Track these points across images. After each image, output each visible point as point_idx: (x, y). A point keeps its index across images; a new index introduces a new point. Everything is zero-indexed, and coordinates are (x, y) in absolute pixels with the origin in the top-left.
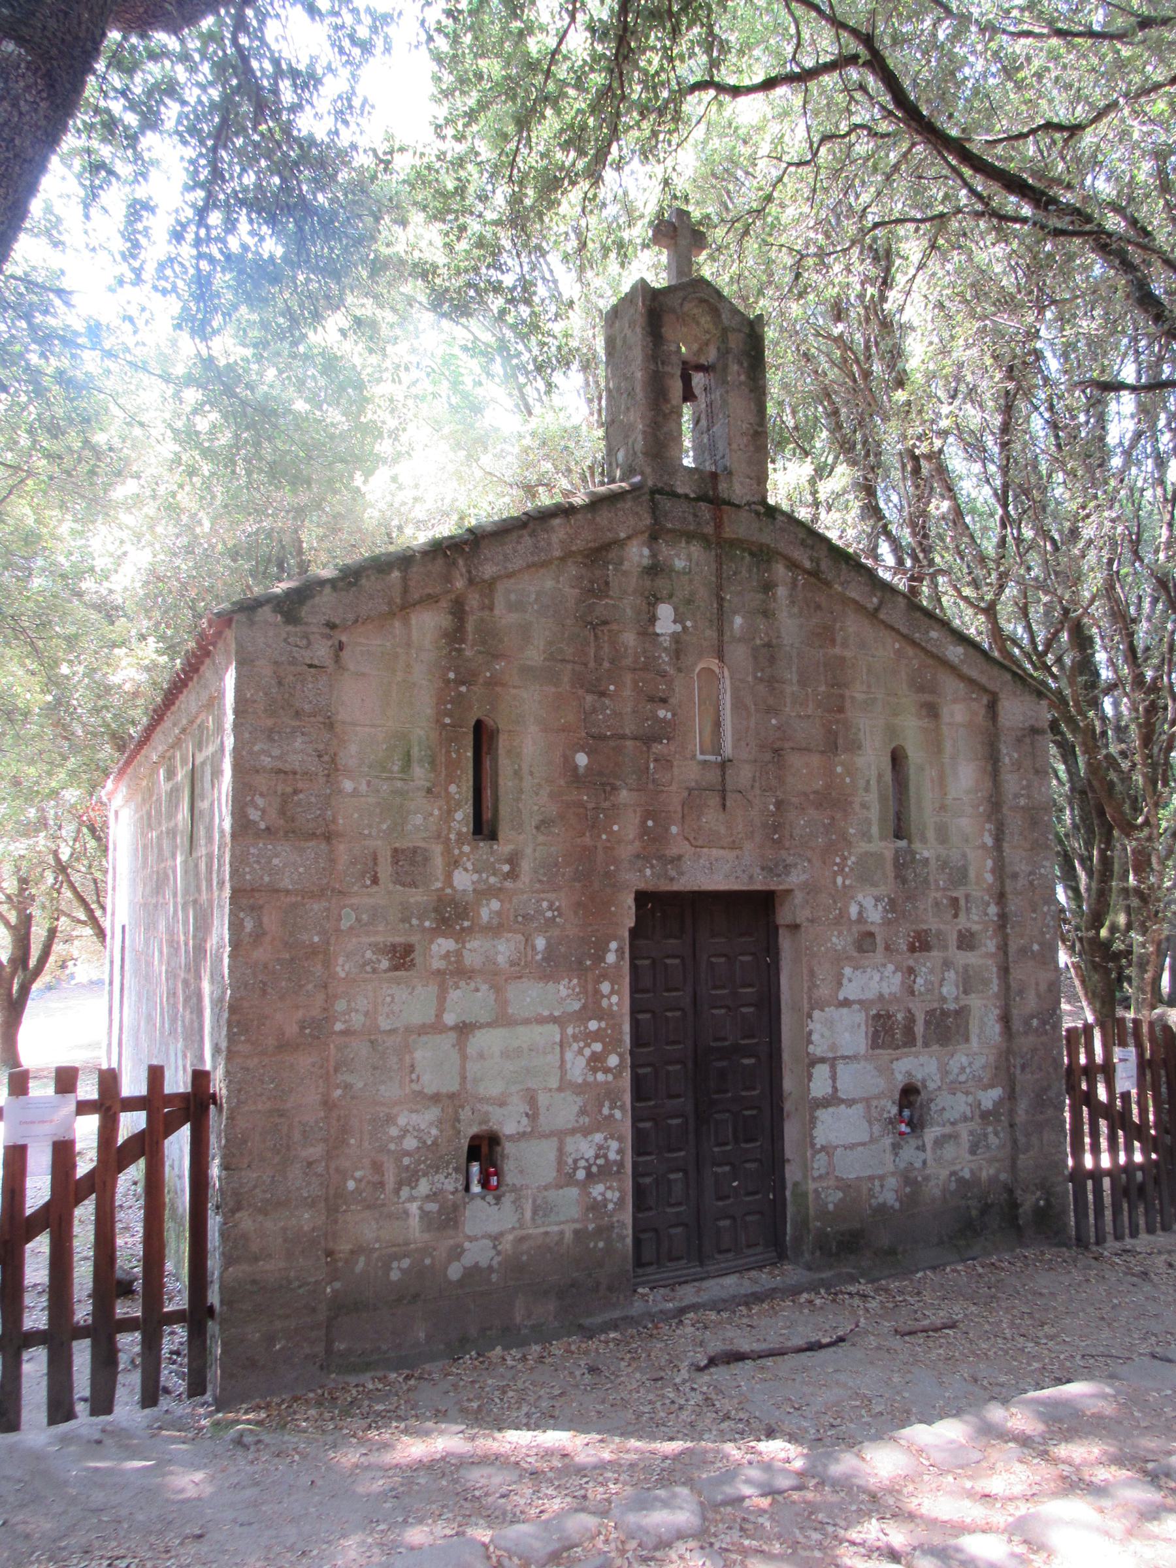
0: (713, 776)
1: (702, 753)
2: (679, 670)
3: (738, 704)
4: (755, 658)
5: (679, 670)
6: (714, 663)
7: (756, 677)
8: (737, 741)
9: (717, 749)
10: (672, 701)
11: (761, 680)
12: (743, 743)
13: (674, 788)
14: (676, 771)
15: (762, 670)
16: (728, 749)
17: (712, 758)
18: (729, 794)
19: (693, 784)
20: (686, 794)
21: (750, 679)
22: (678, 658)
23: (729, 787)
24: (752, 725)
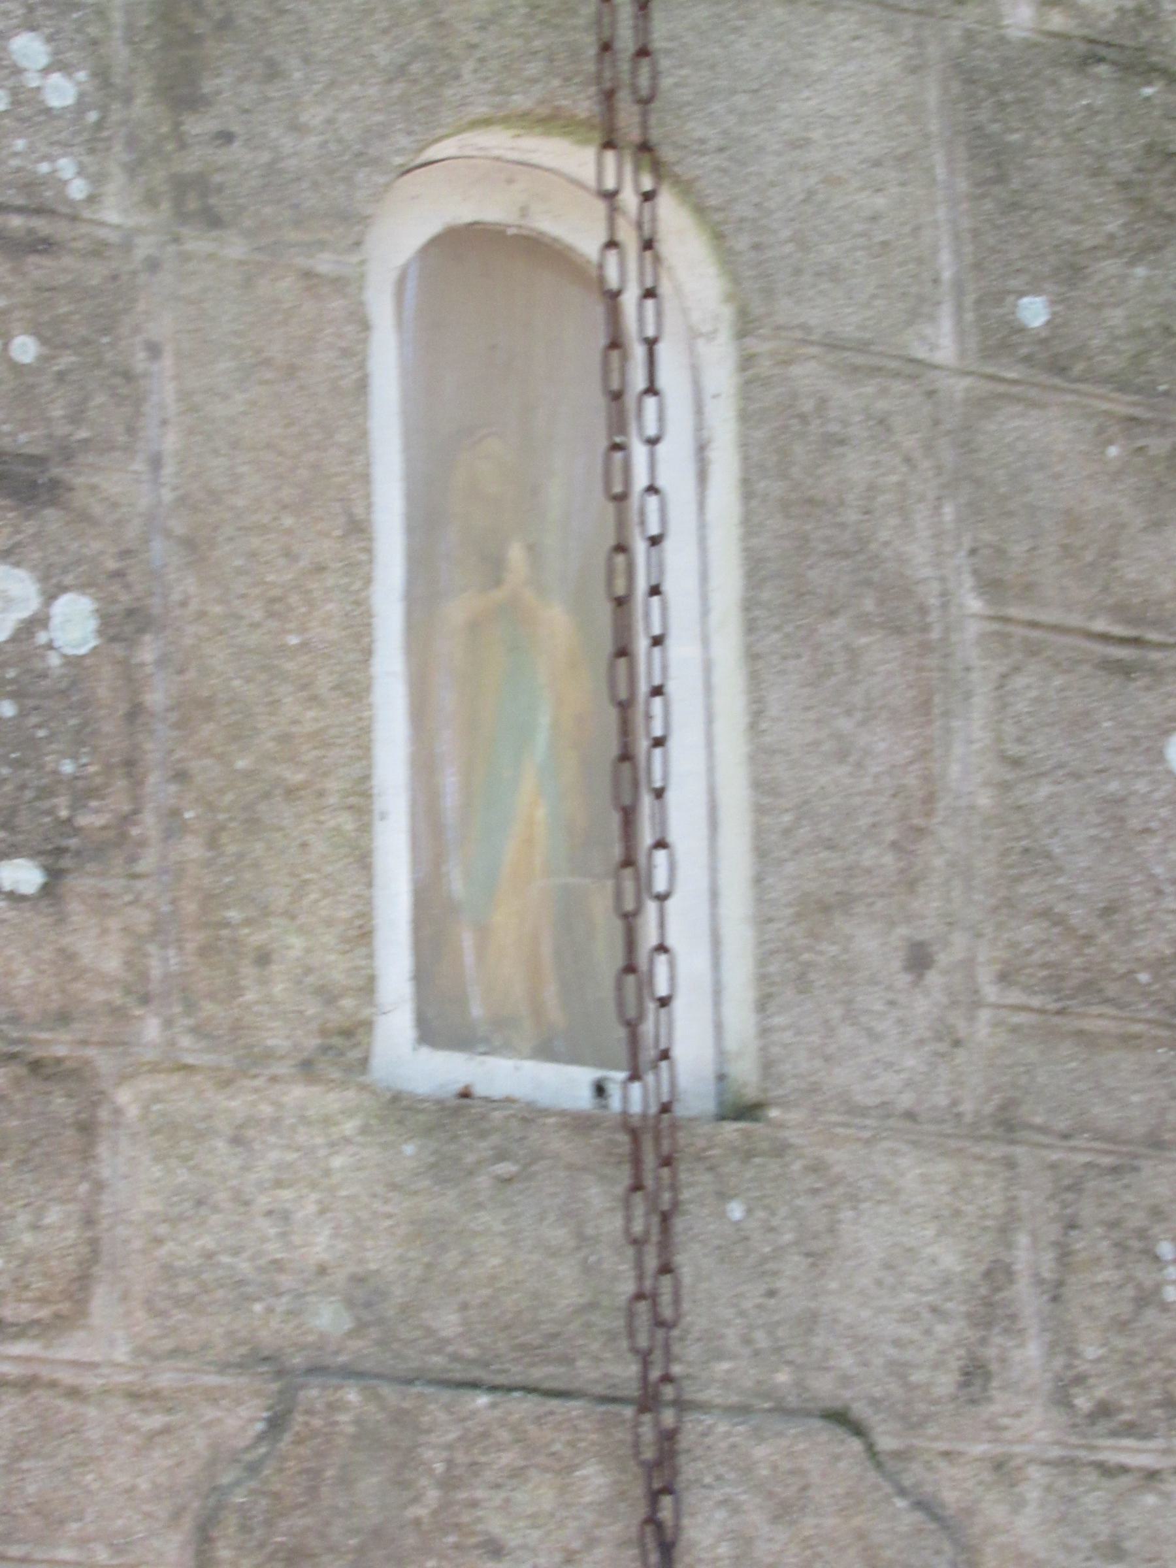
0: (548, 1256)
1: (430, 1033)
2: (196, 203)
3: (807, 572)
4: (992, 162)
5: (196, 203)
6: (556, 182)
7: (999, 339)
8: (802, 928)
9: (627, 1013)
10: (117, 485)
11: (1055, 359)
12: (872, 944)
13: (107, 1341)
14: (134, 1179)
15: (1069, 273)
16: (707, 1025)
17: (567, 1084)
18: (710, 1440)
19: (328, 1318)
20: (242, 1420)
21: (942, 341)
22: (182, 92)
23: (721, 1351)
24: (967, 765)
